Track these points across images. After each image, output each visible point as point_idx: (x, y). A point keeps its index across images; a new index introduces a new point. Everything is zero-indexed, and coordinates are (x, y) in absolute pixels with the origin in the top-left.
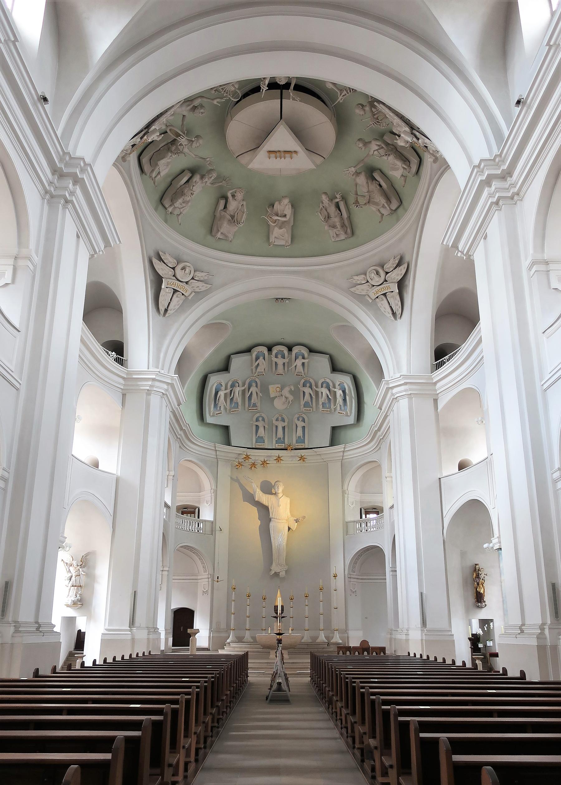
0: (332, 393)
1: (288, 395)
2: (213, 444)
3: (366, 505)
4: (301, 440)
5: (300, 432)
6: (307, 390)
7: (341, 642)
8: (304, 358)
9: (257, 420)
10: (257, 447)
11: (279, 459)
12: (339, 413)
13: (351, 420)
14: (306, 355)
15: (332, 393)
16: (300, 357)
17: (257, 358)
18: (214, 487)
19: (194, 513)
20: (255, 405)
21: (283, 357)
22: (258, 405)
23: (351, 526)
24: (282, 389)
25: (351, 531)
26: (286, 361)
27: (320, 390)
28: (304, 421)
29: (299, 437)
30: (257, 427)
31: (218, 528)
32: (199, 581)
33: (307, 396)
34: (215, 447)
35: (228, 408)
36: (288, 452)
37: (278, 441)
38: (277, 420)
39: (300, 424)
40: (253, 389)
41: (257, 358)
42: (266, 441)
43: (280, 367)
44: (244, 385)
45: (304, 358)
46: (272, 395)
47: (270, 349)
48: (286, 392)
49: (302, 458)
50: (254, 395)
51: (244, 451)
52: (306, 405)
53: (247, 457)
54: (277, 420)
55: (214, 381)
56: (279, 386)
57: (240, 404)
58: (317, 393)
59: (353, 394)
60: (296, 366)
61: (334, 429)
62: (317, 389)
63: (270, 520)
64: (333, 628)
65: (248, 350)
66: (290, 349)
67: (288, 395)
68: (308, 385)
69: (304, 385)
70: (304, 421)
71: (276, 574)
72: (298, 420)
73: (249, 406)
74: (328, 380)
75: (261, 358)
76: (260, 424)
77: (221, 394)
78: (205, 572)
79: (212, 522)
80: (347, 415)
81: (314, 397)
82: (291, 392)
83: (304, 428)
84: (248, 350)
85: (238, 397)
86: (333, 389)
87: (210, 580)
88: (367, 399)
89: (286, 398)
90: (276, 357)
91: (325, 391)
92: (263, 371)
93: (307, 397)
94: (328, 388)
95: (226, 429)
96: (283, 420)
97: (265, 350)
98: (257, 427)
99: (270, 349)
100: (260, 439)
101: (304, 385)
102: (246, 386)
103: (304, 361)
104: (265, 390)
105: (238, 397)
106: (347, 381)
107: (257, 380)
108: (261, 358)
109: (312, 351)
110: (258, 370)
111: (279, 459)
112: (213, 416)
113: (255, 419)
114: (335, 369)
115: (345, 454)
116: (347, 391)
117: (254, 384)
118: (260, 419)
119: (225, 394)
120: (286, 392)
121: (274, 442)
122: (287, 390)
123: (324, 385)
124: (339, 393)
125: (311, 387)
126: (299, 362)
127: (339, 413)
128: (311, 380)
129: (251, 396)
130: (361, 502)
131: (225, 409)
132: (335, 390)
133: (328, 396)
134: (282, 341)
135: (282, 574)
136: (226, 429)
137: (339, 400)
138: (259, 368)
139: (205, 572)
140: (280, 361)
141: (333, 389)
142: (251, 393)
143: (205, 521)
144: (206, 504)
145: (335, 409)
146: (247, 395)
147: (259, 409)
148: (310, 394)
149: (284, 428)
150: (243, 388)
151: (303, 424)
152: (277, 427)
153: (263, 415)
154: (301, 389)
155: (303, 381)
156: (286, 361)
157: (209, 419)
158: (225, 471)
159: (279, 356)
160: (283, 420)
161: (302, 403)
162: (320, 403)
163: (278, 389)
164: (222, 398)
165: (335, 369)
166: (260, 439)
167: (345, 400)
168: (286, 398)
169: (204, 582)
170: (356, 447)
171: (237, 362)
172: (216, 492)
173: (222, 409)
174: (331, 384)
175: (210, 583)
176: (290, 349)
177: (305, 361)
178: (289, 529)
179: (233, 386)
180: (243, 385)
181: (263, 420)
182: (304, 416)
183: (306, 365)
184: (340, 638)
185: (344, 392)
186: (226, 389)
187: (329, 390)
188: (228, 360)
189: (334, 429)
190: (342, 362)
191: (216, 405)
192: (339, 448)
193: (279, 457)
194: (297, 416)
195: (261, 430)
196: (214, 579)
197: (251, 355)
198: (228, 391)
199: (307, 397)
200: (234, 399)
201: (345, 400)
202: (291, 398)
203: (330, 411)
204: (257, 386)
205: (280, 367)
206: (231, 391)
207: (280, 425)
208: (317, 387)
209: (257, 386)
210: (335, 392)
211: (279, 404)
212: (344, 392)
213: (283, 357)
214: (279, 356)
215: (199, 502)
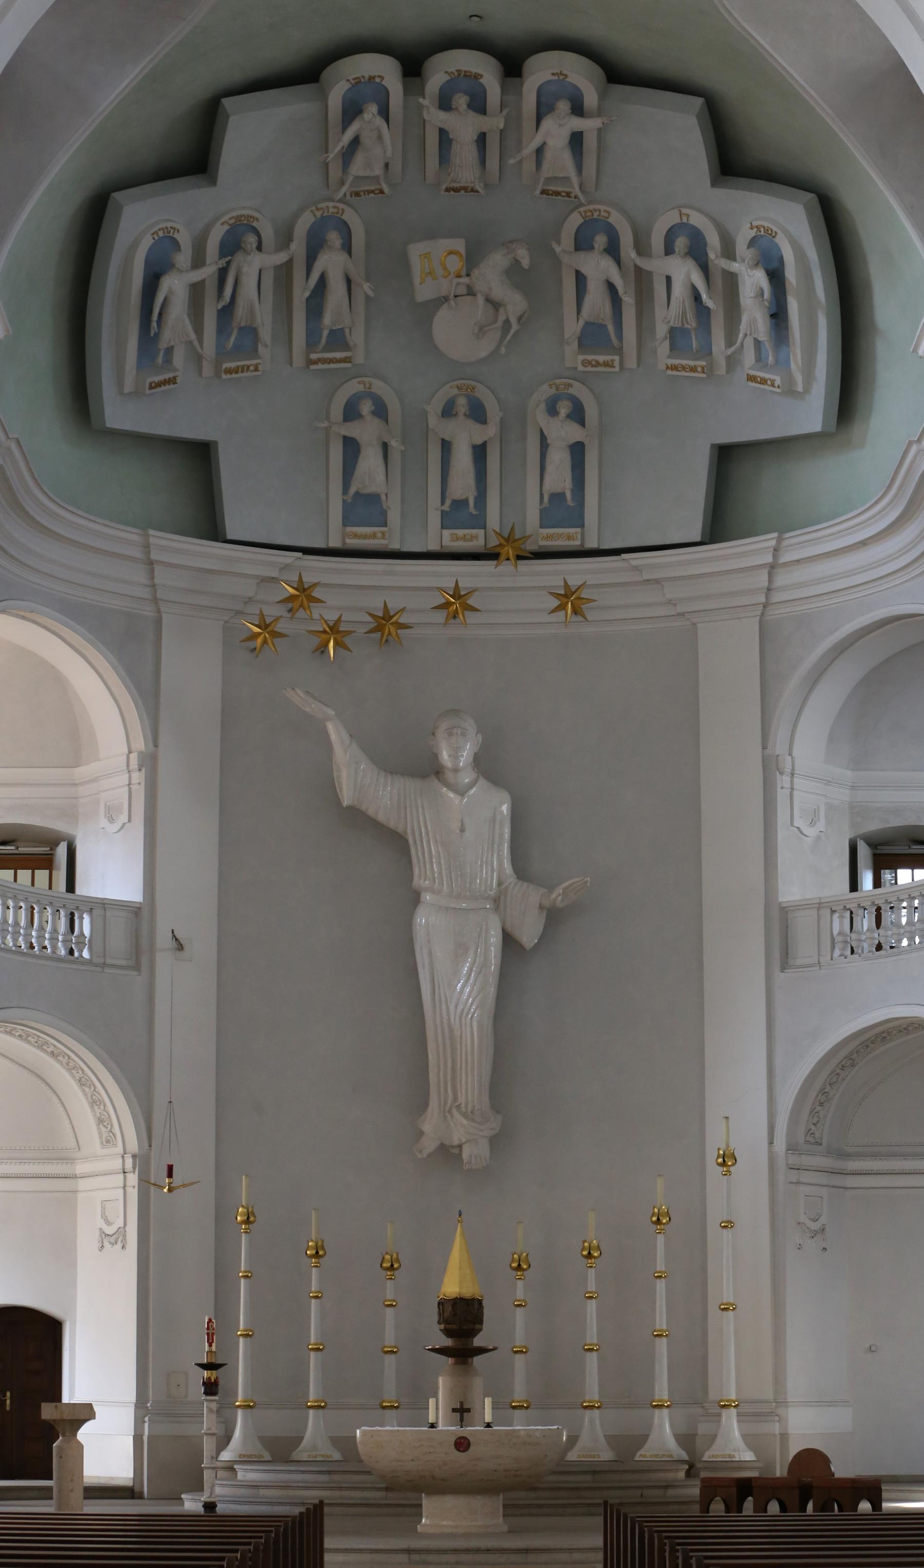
0: (718, 281)
1: (500, 291)
2: (133, 535)
4: (564, 509)
5: (559, 475)
6: (597, 267)
7: (748, 1456)
8: (578, 109)
9: (351, 413)
10: (353, 543)
11: (457, 604)
12: (751, 378)
13: (811, 413)
14: (591, 98)
15: (718, 281)
16: (563, 106)
17: (351, 112)
18: (140, 744)
19: (47, 862)
20: (338, 340)
21: (479, 105)
22: (357, 337)
23: (804, 923)
24: (473, 258)
25: (805, 949)
26: (494, 123)
27: (659, 265)
28: (578, 415)
29: (558, 497)
30: (351, 448)
31: (163, 940)
32: (82, 1184)
34: (147, 547)
36: (506, 567)
37: (456, 514)
38: (448, 411)
39: (562, 432)
40: (331, 262)
41: (351, 112)
42: (394, 516)
43: (464, 153)
44: (285, 239)
45: (578, 109)
46: (424, 292)
47: (413, 66)
49: (570, 600)
50: (336, 291)
51: (285, 568)
52: (593, 337)
53: (304, 595)
54: (448, 411)
55: (139, 222)
56: (459, 245)
57: (265, 334)
59: (822, 287)
60: (540, 151)
61: (726, 456)
62: (644, 264)
63: (415, 898)
64: (713, 1395)
65: (308, 73)
66: (512, 65)
67: (500, 291)
68: (601, 241)
69: (582, 243)
70: (578, 415)
71: (448, 1154)
72: (552, 411)
73: (311, 344)
74: (697, 220)
75: (372, 110)
76: (367, 431)
77: (175, 285)
78: (108, 1142)
79: (135, 910)
80: (790, 391)
81: (628, 301)
83: (577, 451)
84: (308, 73)
86: (724, 263)
87: (133, 1179)
90: (445, 104)
91: (683, 272)
92: (378, 171)
93: (596, 302)
94: (697, 253)
95: (200, 456)
96: (478, 413)
97: (385, 69)
98: (351, 448)
99: (413, 66)
100: (364, 507)
102: (298, 247)
103: (577, 123)
106: (789, 223)
107: (350, 216)
108: (372, 110)
109: (617, 74)
110: (358, 168)
111: (457, 604)
112: (137, 393)
113: (337, 410)
114: (732, 162)
115: (781, 579)
116: (791, 274)
117: (334, 238)
118: (366, 408)
119: (196, 290)
120: (491, 274)
121: (434, 519)
123: (681, 243)
124: (753, 281)
125: (613, 250)
126: (556, 130)
127: (751, 378)
128: (616, 219)
130: (856, 811)
131: (197, 359)
132: (735, 267)
133: (697, 297)
134: (474, 26)
135: (476, 1152)
136: (200, 456)
137: (754, 316)
138: (359, 159)
139: (108, 1142)
140: (464, 126)
141: (724, 263)
142: (323, 279)
143: (104, 904)
144: (104, 822)
145: (732, 362)
146: (301, 291)
147: (360, 358)
148: (611, 287)
149: (480, 452)
150: (281, 258)
151: (574, 433)
152: (446, 447)
153: (379, 387)
154: (565, 259)
155: (575, 220)
156: (494, 123)
157: (117, 412)
158: (196, 667)
159: (461, 101)
160: (478, 413)
161: (572, 328)
162: (661, 330)
163: (455, 264)
165: (732, 162)
166: (364, 507)
167: (778, 316)
168: (495, 305)
169: (106, 1191)
171: (254, 133)
172: (150, 763)
173: (179, 359)
174: (713, 240)
175: (133, 1194)
176: (512, 65)
177: (588, 125)
178: (509, 941)
179: (231, 246)
181: (381, 411)
182: (578, 390)
183: (590, 143)
184: (750, 1440)
185: (776, 276)
186: (198, 262)
187: (705, 268)
188: (208, 120)
189: (726, 456)
190: (765, 127)
192: (746, 553)
193: (456, 595)
194: (546, 391)
195: (370, 462)
196: (156, 1177)
197: (323, 97)
198: (208, 272)
199: (596, 297)
200: (240, 312)
201: (778, 316)
202: (515, 303)
203: (709, 370)
204: (347, 248)
205: (464, 153)
206: (222, 274)
207: (464, 436)
208: (642, 248)
209: (347, 248)
211: (455, 333)
212: (776, 276)
213: (479, 105)
214: (461, 101)
215: (71, 813)
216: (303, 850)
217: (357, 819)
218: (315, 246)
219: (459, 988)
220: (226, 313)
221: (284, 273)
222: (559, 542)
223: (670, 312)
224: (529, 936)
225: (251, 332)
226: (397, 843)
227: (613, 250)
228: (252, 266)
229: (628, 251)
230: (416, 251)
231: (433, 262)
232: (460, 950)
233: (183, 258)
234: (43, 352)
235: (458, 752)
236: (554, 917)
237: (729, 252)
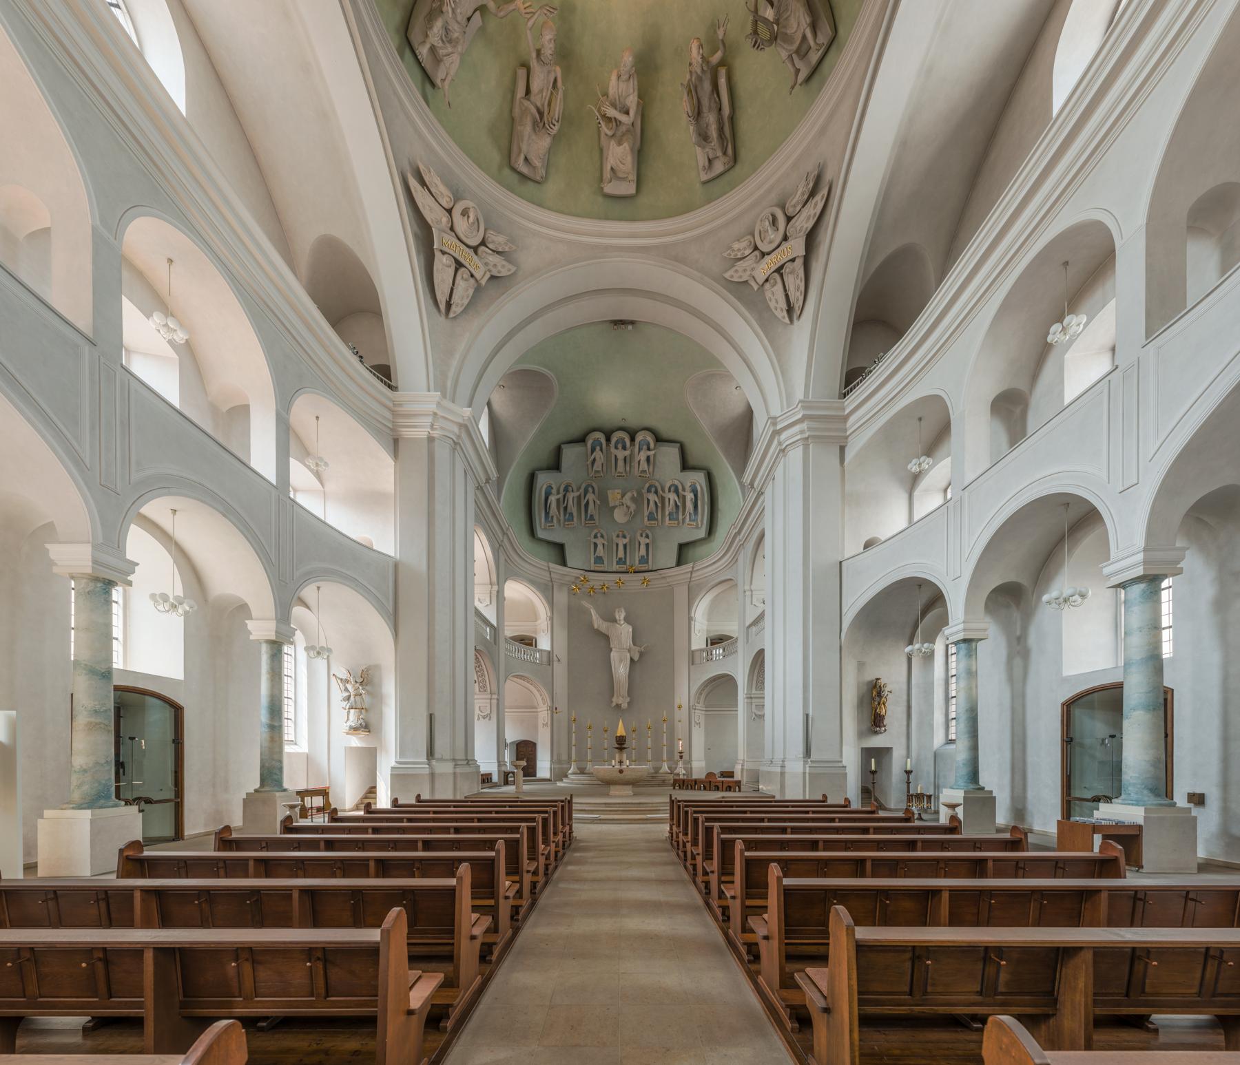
1: (629, 503)
3: (711, 634)
6: (653, 497)
20: (592, 518)
22: (596, 517)
26: (627, 453)
33: (652, 503)
35: (562, 518)
40: (590, 497)
48: (627, 499)
50: (591, 505)
52: (651, 517)
57: (575, 514)
58: (663, 499)
67: (629, 503)
69: (649, 491)
77: (553, 499)
82: (633, 499)
85: (573, 508)
88: (722, 504)
89: (628, 507)
91: (673, 496)
101: (649, 491)
102: (582, 490)
104: (604, 499)
105: (573, 508)
119: (558, 500)
122: (629, 495)
125: (656, 492)
129: (587, 506)
131: (559, 521)
145: (684, 520)
161: (646, 513)
163: (619, 496)
164: (554, 505)
167: (696, 507)
168: (628, 507)
170: (710, 562)
174: (680, 488)
179: (566, 490)
180: (578, 490)
185: (696, 496)
191: (547, 514)
192: (687, 568)
198: (561, 496)
201: (696, 507)
202: (633, 507)
208: (663, 490)
210: (684, 497)
211: (619, 516)
212: (696, 496)
216: (588, 641)
217: (598, 633)
218: (586, 492)
219: (621, 670)
220: (565, 508)
221: (579, 497)
222: (644, 568)
223: (669, 508)
224: (636, 658)
225: (571, 514)
226: (606, 638)
227: (656, 492)
228: (571, 496)
229: (660, 492)
230: (609, 492)
231: (614, 496)
232: (621, 661)
233: (554, 491)
234: (522, 516)
235: (621, 615)
236: (641, 654)
237: (684, 490)
